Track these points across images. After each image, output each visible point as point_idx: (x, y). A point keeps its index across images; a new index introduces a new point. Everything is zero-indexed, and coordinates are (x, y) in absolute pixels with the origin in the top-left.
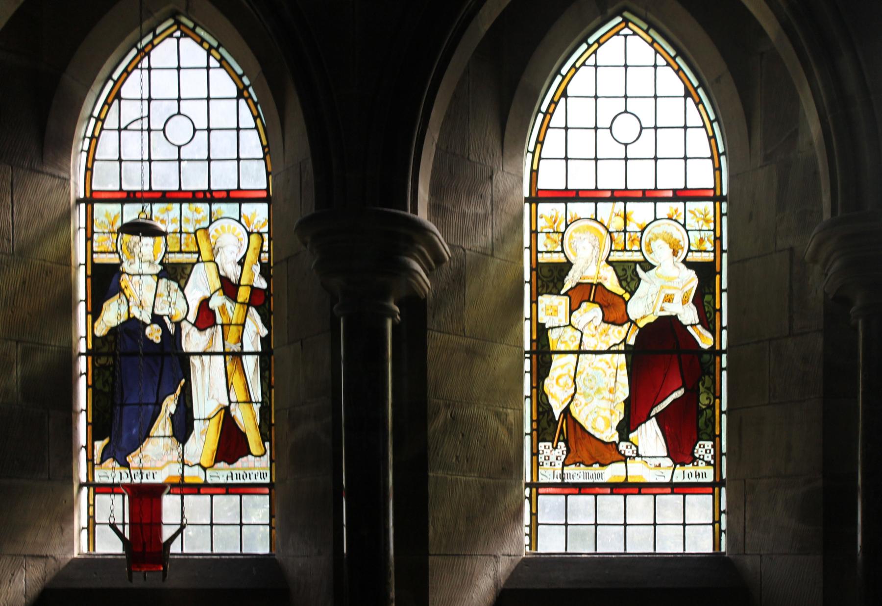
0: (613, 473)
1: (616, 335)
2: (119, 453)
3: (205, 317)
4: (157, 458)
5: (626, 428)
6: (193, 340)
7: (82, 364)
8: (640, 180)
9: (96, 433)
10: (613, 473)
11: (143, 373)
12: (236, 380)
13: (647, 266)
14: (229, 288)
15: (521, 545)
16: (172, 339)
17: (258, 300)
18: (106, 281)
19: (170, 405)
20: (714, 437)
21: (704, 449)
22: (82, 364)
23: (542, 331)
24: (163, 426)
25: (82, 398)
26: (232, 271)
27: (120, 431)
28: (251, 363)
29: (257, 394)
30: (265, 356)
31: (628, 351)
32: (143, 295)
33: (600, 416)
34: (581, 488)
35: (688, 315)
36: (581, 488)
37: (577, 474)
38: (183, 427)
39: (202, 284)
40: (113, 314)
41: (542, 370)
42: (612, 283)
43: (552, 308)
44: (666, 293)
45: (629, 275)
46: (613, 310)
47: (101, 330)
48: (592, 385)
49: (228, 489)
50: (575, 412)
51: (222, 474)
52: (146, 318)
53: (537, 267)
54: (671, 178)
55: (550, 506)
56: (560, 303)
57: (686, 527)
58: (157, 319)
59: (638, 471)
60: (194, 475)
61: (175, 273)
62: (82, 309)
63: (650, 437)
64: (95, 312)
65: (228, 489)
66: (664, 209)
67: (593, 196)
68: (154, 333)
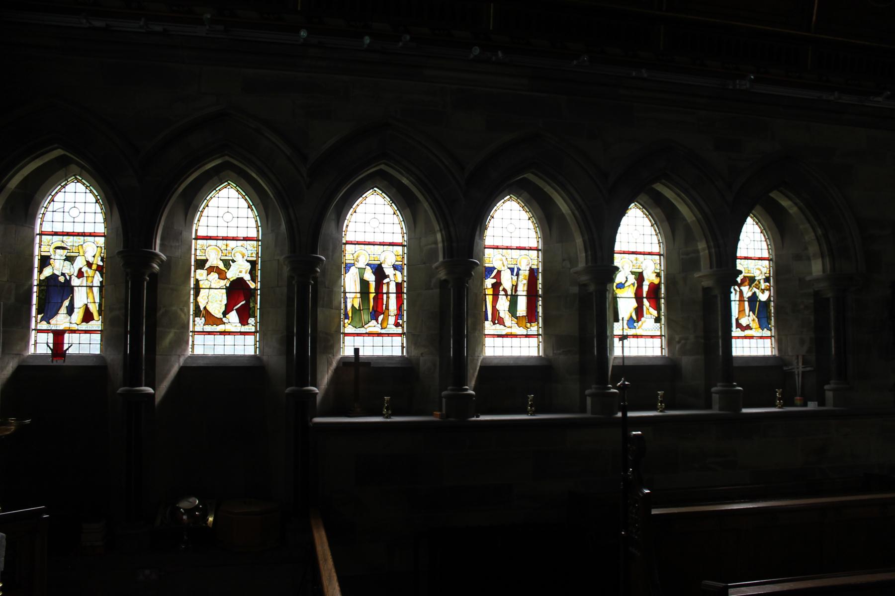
0: (221, 328)
2: (47, 319)
3: (80, 274)
4: (61, 321)
5: (225, 314)
6: (75, 282)
7: (35, 289)
9: (39, 312)
10: (221, 328)
11: (57, 292)
12: (90, 295)
13: (234, 261)
14: (89, 265)
15: (189, 352)
16: (68, 282)
17: (99, 269)
18: (45, 261)
19: (66, 303)
20: (255, 317)
21: (251, 321)
22: (35, 289)
23: (197, 281)
24: (63, 310)
26: (91, 260)
27: (48, 310)
28: (96, 290)
29: (97, 300)
30: (101, 288)
31: (227, 288)
32: (58, 266)
33: (217, 309)
34: (209, 333)
35: (247, 277)
36: (209, 333)
37: (208, 328)
38: (70, 310)
39: (80, 263)
40: (47, 272)
41: (197, 294)
42: (221, 266)
43: (201, 274)
44: (240, 270)
45: (227, 264)
46: (222, 275)
47: (42, 277)
48: (213, 298)
49: (86, 332)
51: (84, 327)
53: (196, 261)
54: (242, 234)
55: (199, 339)
56: (205, 272)
58: (63, 274)
59: (228, 328)
60: (74, 327)
62: (36, 271)
63: (233, 316)
64: (40, 272)
65: (86, 332)
67: (216, 238)
68: (62, 279)
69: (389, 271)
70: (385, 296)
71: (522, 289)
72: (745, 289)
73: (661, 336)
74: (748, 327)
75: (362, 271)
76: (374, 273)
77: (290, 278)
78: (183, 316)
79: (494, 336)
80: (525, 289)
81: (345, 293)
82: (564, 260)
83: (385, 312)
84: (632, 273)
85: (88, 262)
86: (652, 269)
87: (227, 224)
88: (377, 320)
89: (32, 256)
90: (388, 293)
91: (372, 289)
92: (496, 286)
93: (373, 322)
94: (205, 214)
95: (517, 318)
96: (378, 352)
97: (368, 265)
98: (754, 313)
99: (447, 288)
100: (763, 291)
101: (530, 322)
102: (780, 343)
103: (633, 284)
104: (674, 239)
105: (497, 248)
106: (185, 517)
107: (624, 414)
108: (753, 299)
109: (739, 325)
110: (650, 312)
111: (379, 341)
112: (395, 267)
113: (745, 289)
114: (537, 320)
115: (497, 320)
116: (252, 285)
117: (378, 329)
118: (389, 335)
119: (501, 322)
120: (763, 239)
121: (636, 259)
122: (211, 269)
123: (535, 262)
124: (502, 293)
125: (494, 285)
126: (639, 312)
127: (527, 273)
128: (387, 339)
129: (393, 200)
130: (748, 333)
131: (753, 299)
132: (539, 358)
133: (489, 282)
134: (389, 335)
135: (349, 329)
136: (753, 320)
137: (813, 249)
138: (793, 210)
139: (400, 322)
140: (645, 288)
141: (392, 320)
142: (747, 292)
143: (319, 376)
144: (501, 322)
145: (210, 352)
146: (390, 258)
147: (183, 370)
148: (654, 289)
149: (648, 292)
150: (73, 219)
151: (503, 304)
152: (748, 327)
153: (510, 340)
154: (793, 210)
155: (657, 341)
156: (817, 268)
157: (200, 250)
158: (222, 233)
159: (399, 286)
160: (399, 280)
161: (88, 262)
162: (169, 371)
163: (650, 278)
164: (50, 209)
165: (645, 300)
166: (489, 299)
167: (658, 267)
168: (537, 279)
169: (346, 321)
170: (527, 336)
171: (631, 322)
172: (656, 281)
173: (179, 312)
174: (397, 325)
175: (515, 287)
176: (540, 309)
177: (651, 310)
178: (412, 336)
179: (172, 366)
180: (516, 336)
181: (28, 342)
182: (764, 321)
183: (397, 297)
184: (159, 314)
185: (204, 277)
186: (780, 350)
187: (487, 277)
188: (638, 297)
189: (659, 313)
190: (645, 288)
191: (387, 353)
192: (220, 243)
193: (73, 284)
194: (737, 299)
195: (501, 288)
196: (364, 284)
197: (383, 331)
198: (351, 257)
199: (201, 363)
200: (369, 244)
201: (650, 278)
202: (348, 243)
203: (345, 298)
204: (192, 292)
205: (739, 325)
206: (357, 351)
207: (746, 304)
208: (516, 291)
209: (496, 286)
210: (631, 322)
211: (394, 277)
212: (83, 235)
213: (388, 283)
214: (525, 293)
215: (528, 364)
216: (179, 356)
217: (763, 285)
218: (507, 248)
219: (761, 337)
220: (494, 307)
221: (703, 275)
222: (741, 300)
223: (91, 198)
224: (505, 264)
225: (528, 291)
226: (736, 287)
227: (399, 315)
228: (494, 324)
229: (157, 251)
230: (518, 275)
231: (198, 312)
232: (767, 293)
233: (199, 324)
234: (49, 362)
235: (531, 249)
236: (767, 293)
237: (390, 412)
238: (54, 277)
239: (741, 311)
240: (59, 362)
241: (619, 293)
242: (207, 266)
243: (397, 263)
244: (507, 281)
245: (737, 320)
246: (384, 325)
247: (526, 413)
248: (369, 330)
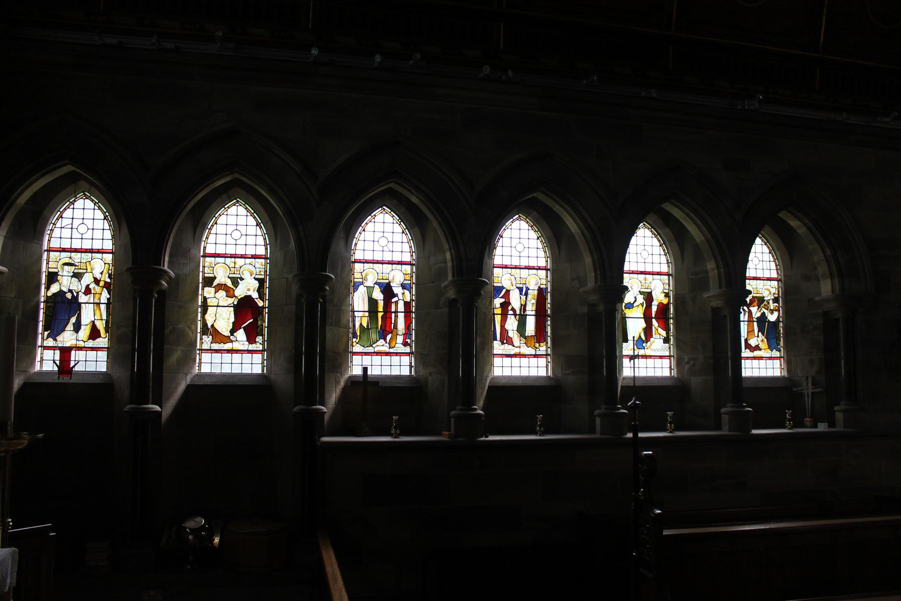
0: (228, 346)
1: (230, 301)
3: (88, 291)
4: (67, 338)
5: (233, 332)
6: (83, 298)
7: (42, 305)
8: (240, 251)
9: (46, 328)
10: (228, 346)
11: (64, 309)
12: (97, 312)
13: (242, 279)
14: (97, 281)
16: (75, 299)
17: (107, 286)
18: (53, 277)
19: (73, 320)
20: (262, 335)
21: (259, 339)
23: (205, 299)
24: (70, 327)
25: (41, 316)
26: (98, 276)
27: (54, 327)
28: (103, 307)
29: (104, 317)
30: (108, 304)
31: (234, 306)
32: (66, 283)
33: (224, 327)
34: (217, 351)
35: (255, 295)
36: (217, 351)
37: (216, 346)
38: (77, 327)
39: (87, 279)
40: (55, 288)
41: (205, 312)
42: (229, 284)
43: (209, 292)
44: (248, 288)
45: (235, 281)
46: (230, 293)
47: (49, 294)
48: (221, 317)
49: (92, 349)
50: (216, 326)
51: (91, 344)
52: (65, 290)
53: (204, 278)
54: (251, 251)
55: (206, 357)
57: (251, 364)
58: (70, 291)
59: (236, 346)
60: (81, 344)
61: (78, 276)
62: (43, 286)
63: (241, 334)
65: (92, 349)
66: (248, 261)
67: (224, 256)
68: (69, 296)
69: (397, 290)
70: (393, 315)
71: (531, 309)
72: (754, 310)
73: (670, 356)
74: (757, 348)
75: (370, 290)
76: (382, 292)
77: (299, 296)
78: (190, 333)
79: (502, 356)
80: (534, 308)
82: (573, 280)
83: (393, 331)
84: (641, 293)
85: (95, 279)
86: (660, 289)
87: (236, 241)
88: (385, 340)
89: (39, 272)
90: (396, 312)
91: (381, 308)
92: (505, 305)
93: (382, 342)
94: (213, 231)
95: (525, 338)
96: (386, 372)
97: (376, 283)
98: (763, 334)
99: (455, 307)
100: (772, 312)
101: (539, 342)
102: (789, 363)
103: (642, 304)
104: (683, 260)
105: (506, 267)
106: (191, 537)
107: (635, 435)
108: (762, 320)
109: (748, 346)
110: (659, 333)
111: (387, 361)
112: (403, 286)
113: (754, 310)
114: (545, 340)
115: (506, 339)
116: (260, 304)
117: (386, 349)
118: (397, 354)
119: (510, 341)
120: (772, 259)
121: (645, 279)
122: (220, 287)
123: (544, 282)
124: (511, 312)
125: (502, 304)
126: (648, 332)
127: (536, 292)
128: (396, 359)
129: (402, 219)
130: (757, 353)
131: (762, 320)
132: (547, 378)
133: (498, 302)
134: (397, 354)
135: (357, 348)
136: (762, 341)
137: (822, 269)
138: (802, 230)
139: (409, 341)
140: (654, 309)
141: (400, 339)
142: (756, 312)
143: (327, 396)
144: (510, 341)
145: (217, 370)
146: (397, 277)
147: (189, 387)
148: (663, 309)
149: (657, 312)
150: (82, 234)
151: (512, 324)
152: (757, 348)
153: (519, 360)
154: (802, 230)
155: (666, 362)
156: (826, 288)
157: (208, 266)
158: (231, 250)
159: (407, 305)
160: (408, 299)
161: (95, 279)
162: (176, 388)
163: (659, 297)
164: (58, 225)
165: (654, 320)
166: (498, 319)
167: (667, 287)
168: (546, 299)
170: (536, 356)
171: (640, 342)
172: (665, 301)
173: (187, 329)
174: (405, 344)
175: (524, 307)
176: (549, 329)
177: (660, 330)
178: (420, 356)
179: (179, 384)
180: (524, 356)
181: (35, 359)
182: (773, 341)
183: (405, 317)
184: (167, 331)
185: (212, 295)
186: (789, 371)
187: (495, 296)
188: (647, 317)
189: (668, 333)
190: (654, 309)
191: (396, 372)
192: (228, 261)
193: (81, 300)
194: (746, 319)
195: (510, 308)
196: (373, 303)
197: (392, 350)
199: (208, 381)
200: (378, 262)
201: (659, 297)
202: (356, 261)
203: (354, 317)
204: (200, 310)
205: (748, 346)
206: (365, 370)
207: (755, 324)
208: (525, 310)
209: (505, 305)
210: (640, 343)
211: (403, 296)
212: (91, 251)
213: (396, 303)
214: (533, 313)
215: (537, 384)
216: (186, 374)
217: (772, 306)
218: (516, 267)
219: (770, 358)
220: (503, 327)
221: (712, 296)
222: (750, 320)
223: (99, 215)
224: (514, 283)
225: (536, 311)
226: (745, 308)
227: (407, 334)
228: (503, 343)
229: (166, 268)
230: (526, 294)
231: (205, 330)
232: (776, 314)
233: (207, 342)
234: (55, 379)
235: (539, 268)
236: (776, 314)
237: (398, 431)
238: (61, 293)
239: (750, 331)
240: (65, 379)
241: (628, 313)
242: (215, 283)
244: (515, 301)
245: (746, 340)
246: (393, 345)
247: (535, 433)
248: (377, 349)
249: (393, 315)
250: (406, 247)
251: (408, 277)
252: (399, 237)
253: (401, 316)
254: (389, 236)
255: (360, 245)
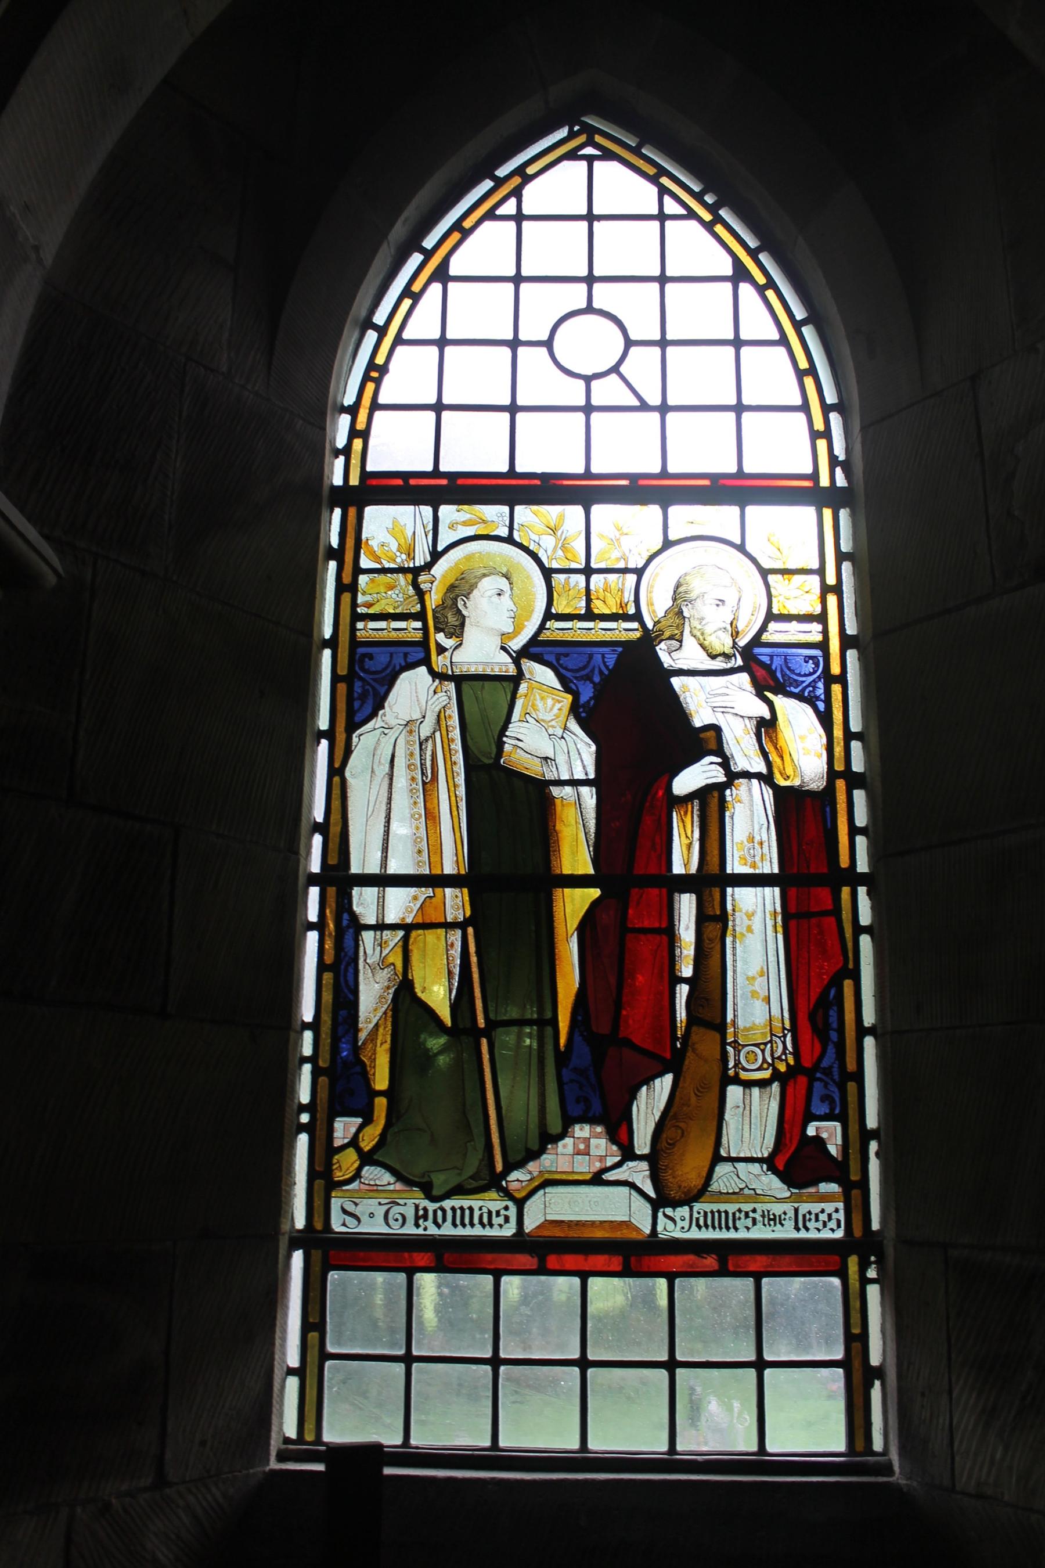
70: (686, 905)
75: (484, 703)
76: (586, 715)
81: (339, 879)
83: (696, 1047)
88: (620, 1131)
90: (712, 881)
91: (575, 855)
93: (585, 1145)
97: (536, 649)
112: (764, 668)
117: (620, 1206)
118: (727, 1258)
134: (727, 1258)
135: (373, 1207)
139: (831, 1134)
141: (751, 1121)
159: (800, 813)
169: (344, 1128)
196: (506, 806)
197: (678, 1225)
198: (395, 595)
203: (344, 930)
213: (711, 802)
227: (814, 1075)
243: (777, 633)
246: (688, 1169)
249: (686, 905)
250: (772, 375)
251: (800, 595)
252: (703, 310)
253: (756, 909)
254: (637, 307)
255: (409, 375)
